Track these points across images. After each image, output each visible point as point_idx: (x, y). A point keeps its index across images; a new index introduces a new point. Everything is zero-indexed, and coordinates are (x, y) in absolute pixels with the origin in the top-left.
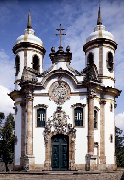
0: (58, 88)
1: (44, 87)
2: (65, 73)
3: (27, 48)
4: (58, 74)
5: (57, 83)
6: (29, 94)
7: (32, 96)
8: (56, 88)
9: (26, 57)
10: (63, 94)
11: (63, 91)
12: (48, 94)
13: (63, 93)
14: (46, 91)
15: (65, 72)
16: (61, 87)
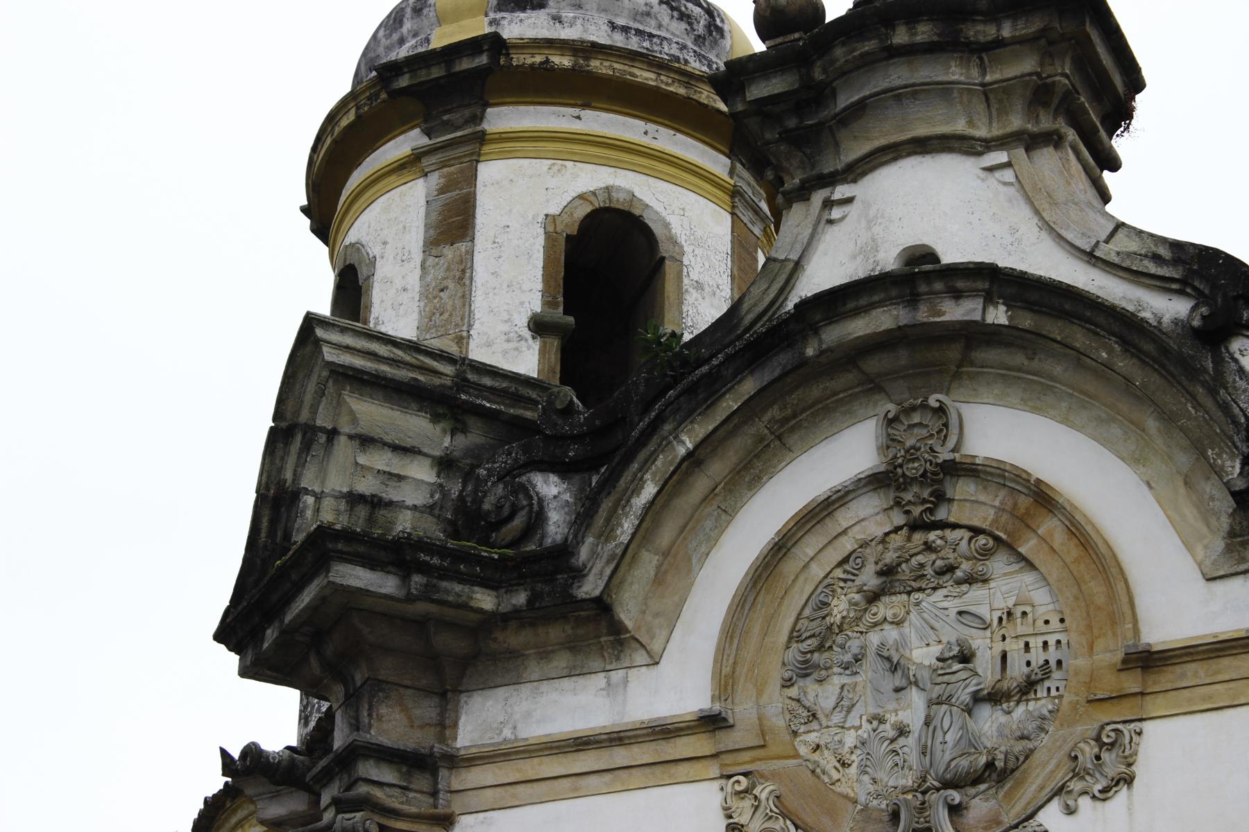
0: (884, 609)
1: (627, 614)
2: (998, 315)
3: (478, 118)
4: (874, 365)
5: (869, 518)
6: (369, 769)
7: (417, 803)
8: (840, 607)
9: (449, 252)
10: (995, 697)
11: (985, 648)
12: (711, 722)
13: (986, 669)
14: (674, 683)
15: (989, 300)
16: (951, 569)
